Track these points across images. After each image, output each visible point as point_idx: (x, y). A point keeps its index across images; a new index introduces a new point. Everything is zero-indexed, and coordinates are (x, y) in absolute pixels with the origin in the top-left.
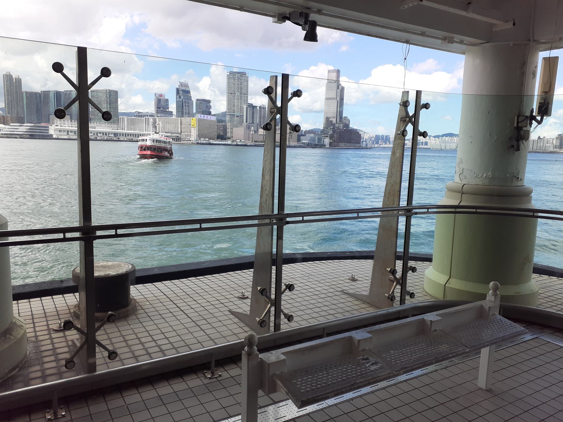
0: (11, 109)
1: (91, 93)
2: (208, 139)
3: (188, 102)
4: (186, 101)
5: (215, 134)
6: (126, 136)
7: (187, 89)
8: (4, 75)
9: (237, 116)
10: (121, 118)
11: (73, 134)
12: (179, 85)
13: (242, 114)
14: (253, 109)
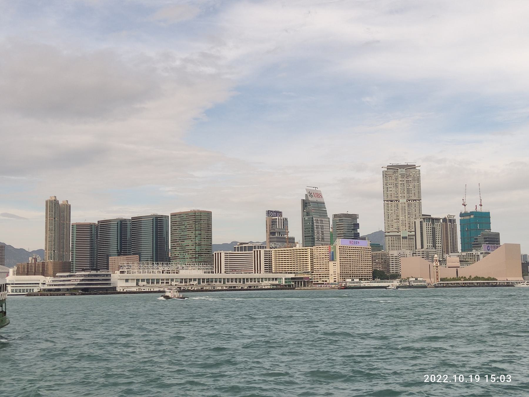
0: (54, 251)
1: (171, 218)
2: (358, 280)
3: (322, 221)
4: (319, 219)
5: (369, 271)
6: (224, 283)
7: (319, 200)
8: (47, 202)
9: (404, 238)
10: (216, 253)
11: (145, 283)
12: (306, 195)
13: (413, 233)
14: (433, 223)
